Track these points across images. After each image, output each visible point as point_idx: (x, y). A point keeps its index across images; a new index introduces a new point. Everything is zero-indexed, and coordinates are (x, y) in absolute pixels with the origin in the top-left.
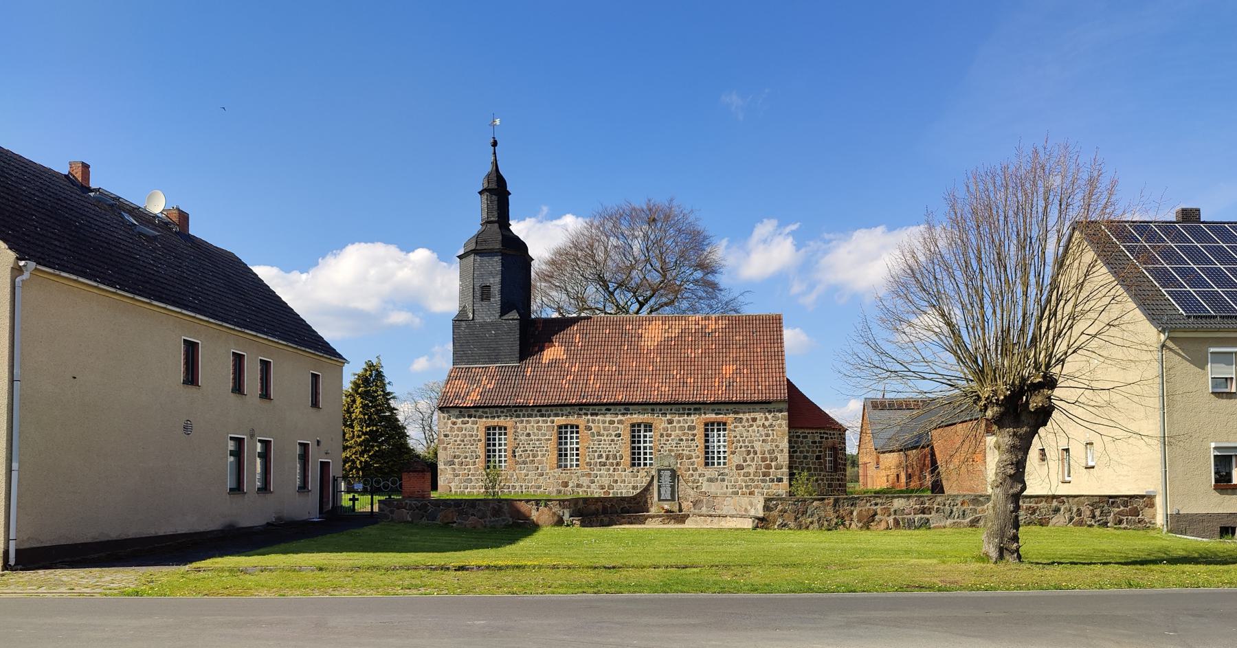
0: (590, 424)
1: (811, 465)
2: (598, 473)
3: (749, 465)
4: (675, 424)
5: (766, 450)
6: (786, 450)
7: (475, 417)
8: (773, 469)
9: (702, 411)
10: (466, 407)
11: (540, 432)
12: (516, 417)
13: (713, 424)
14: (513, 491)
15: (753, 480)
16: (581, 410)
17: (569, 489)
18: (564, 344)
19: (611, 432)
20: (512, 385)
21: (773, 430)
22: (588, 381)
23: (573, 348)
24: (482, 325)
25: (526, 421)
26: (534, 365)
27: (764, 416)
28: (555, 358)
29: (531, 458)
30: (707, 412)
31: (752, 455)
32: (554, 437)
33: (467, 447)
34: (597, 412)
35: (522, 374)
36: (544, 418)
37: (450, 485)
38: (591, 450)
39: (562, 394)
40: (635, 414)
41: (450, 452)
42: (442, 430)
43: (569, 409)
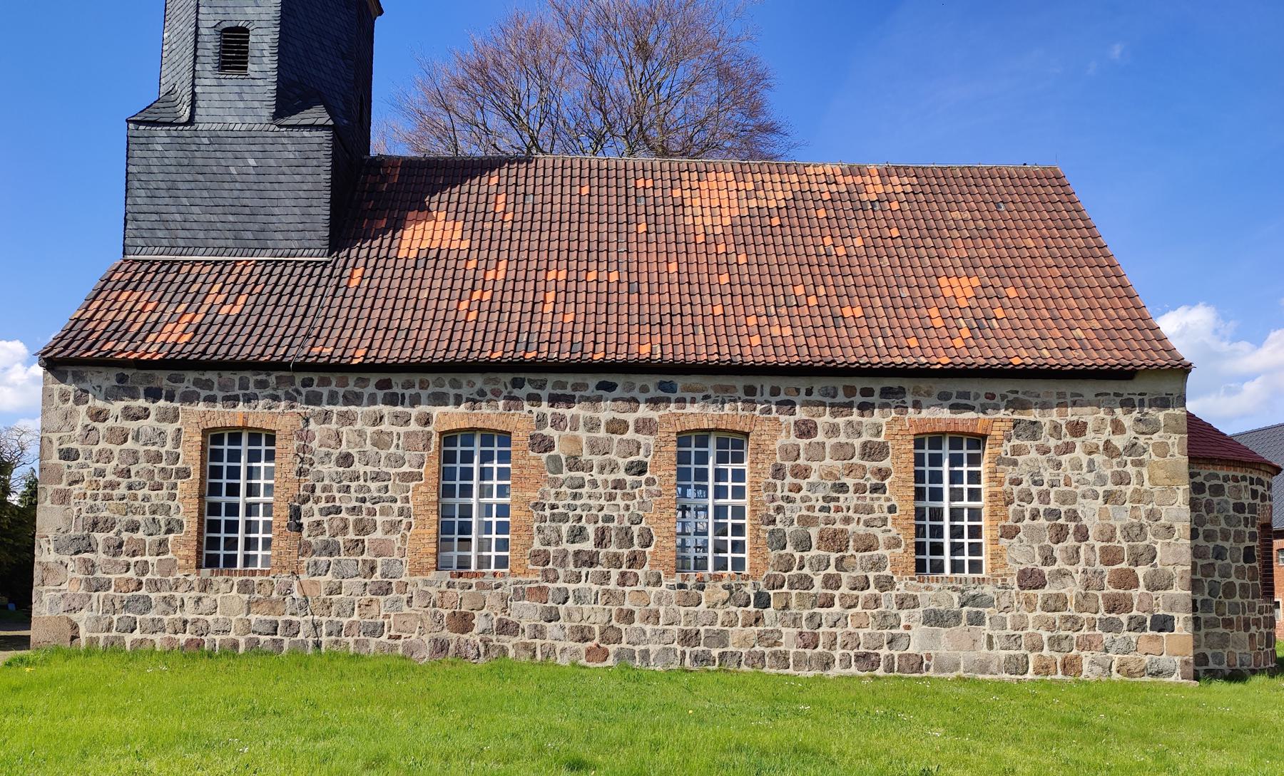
0: (548, 431)
1: (1233, 579)
2: (571, 587)
3: (1062, 574)
4: (820, 437)
5: (1118, 525)
6: (1182, 528)
7: (170, 398)
8: (1142, 589)
9: (909, 399)
10: (139, 364)
11: (383, 453)
12: (308, 402)
13: (936, 440)
14: (287, 641)
15: (1075, 623)
16: (518, 384)
17: (474, 637)
18: (461, 216)
19: (612, 456)
20: (301, 311)
21: (1140, 464)
22: (538, 308)
23: (488, 226)
24: (215, 138)
25: (342, 415)
26: (372, 262)
27: (1109, 418)
28: (435, 245)
29: (351, 535)
30: (923, 400)
31: (1071, 541)
32: (430, 470)
33: (140, 493)
34: (569, 391)
35: (334, 281)
36: (399, 408)
37: (74, 617)
38: (548, 512)
39: (457, 336)
40: (693, 401)
41: (79, 508)
42: (54, 437)
43: (479, 380)
